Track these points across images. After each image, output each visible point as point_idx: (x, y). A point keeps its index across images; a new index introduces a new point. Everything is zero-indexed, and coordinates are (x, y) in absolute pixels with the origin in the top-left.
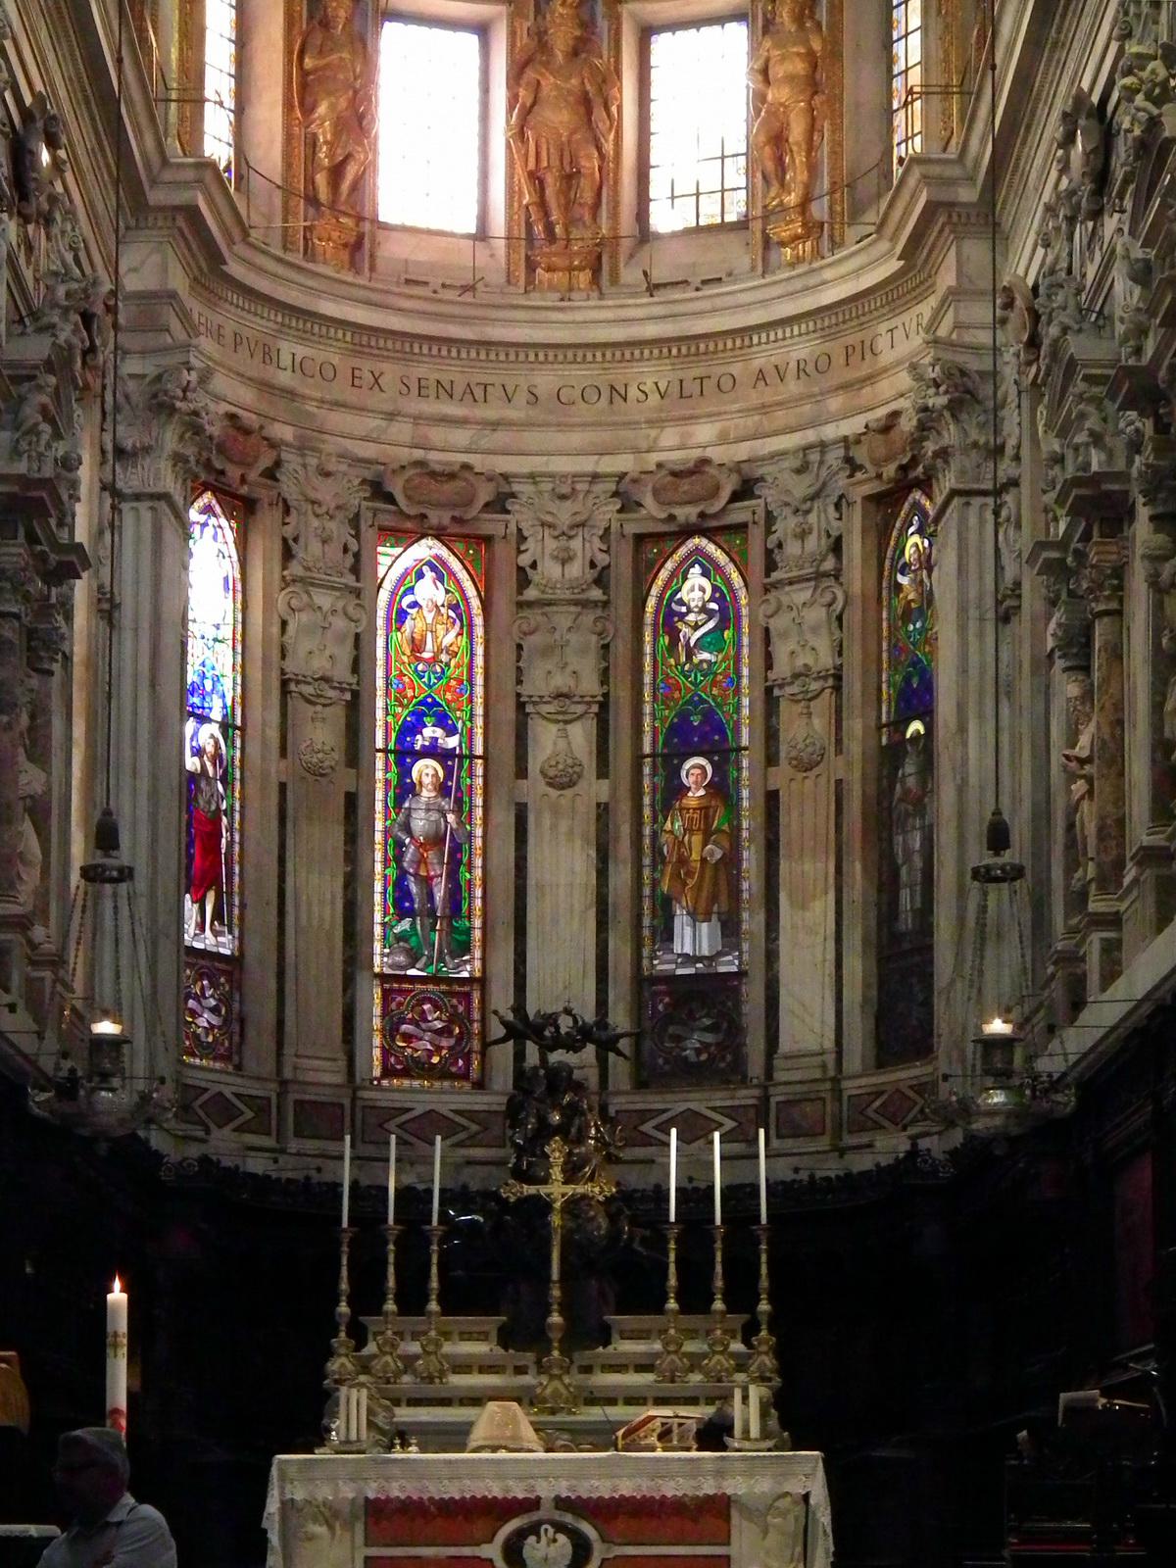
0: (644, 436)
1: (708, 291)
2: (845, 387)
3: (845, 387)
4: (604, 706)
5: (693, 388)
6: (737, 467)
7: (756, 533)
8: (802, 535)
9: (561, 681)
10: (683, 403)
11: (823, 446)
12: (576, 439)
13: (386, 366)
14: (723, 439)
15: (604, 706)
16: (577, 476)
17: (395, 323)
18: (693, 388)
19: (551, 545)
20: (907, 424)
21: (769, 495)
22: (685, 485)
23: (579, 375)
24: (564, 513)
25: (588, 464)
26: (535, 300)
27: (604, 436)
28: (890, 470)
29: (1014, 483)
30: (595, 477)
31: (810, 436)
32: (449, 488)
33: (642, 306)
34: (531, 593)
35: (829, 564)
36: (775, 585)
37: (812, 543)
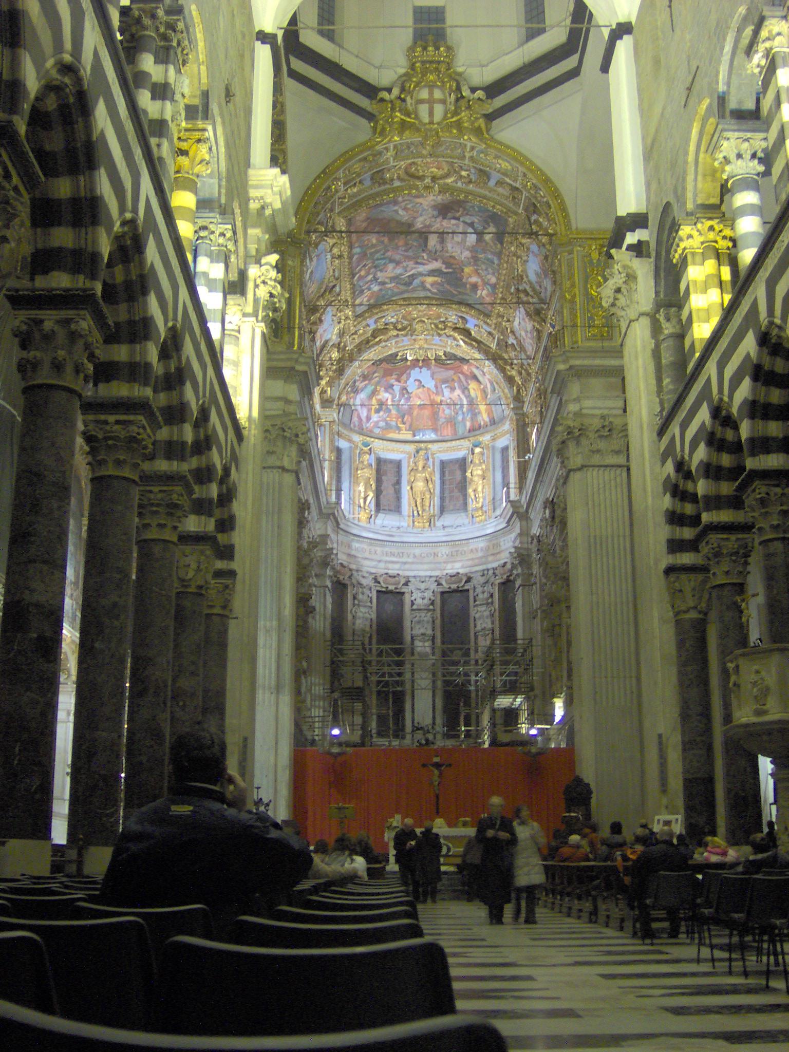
0: (443, 565)
1: (459, 529)
2: (493, 554)
3: (493, 554)
4: (434, 637)
5: (455, 554)
6: (466, 574)
7: (471, 592)
8: (483, 593)
9: (422, 631)
10: (452, 557)
11: (488, 570)
12: (426, 567)
13: (376, 548)
14: (462, 567)
15: (434, 637)
16: (426, 576)
17: (380, 537)
18: (455, 554)
19: (420, 595)
20: (509, 566)
21: (474, 582)
22: (453, 579)
23: (426, 550)
24: (423, 586)
25: (428, 573)
26: (415, 530)
27: (432, 566)
28: (505, 577)
29: (535, 583)
30: (431, 577)
31: (484, 567)
32: (393, 580)
33: (441, 533)
34: (415, 607)
35: (490, 601)
36: (477, 606)
37: (486, 595)
